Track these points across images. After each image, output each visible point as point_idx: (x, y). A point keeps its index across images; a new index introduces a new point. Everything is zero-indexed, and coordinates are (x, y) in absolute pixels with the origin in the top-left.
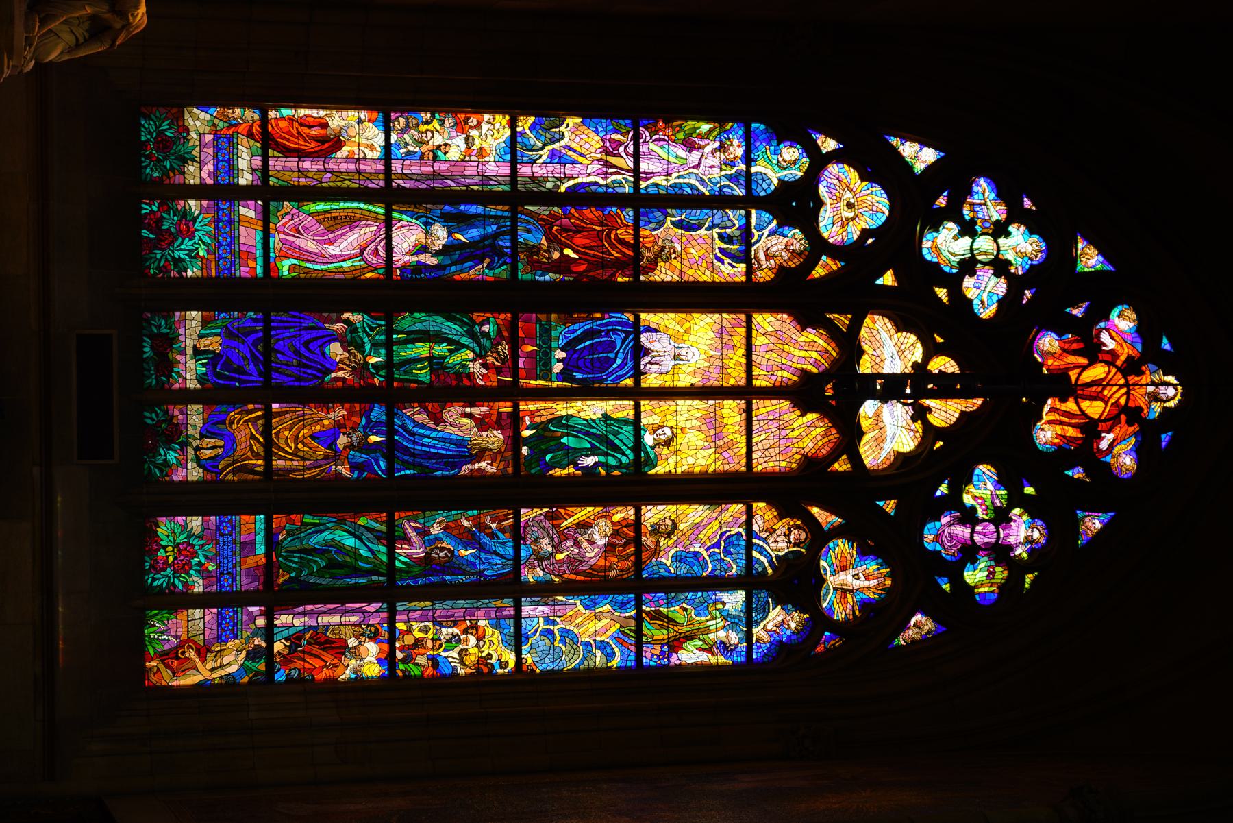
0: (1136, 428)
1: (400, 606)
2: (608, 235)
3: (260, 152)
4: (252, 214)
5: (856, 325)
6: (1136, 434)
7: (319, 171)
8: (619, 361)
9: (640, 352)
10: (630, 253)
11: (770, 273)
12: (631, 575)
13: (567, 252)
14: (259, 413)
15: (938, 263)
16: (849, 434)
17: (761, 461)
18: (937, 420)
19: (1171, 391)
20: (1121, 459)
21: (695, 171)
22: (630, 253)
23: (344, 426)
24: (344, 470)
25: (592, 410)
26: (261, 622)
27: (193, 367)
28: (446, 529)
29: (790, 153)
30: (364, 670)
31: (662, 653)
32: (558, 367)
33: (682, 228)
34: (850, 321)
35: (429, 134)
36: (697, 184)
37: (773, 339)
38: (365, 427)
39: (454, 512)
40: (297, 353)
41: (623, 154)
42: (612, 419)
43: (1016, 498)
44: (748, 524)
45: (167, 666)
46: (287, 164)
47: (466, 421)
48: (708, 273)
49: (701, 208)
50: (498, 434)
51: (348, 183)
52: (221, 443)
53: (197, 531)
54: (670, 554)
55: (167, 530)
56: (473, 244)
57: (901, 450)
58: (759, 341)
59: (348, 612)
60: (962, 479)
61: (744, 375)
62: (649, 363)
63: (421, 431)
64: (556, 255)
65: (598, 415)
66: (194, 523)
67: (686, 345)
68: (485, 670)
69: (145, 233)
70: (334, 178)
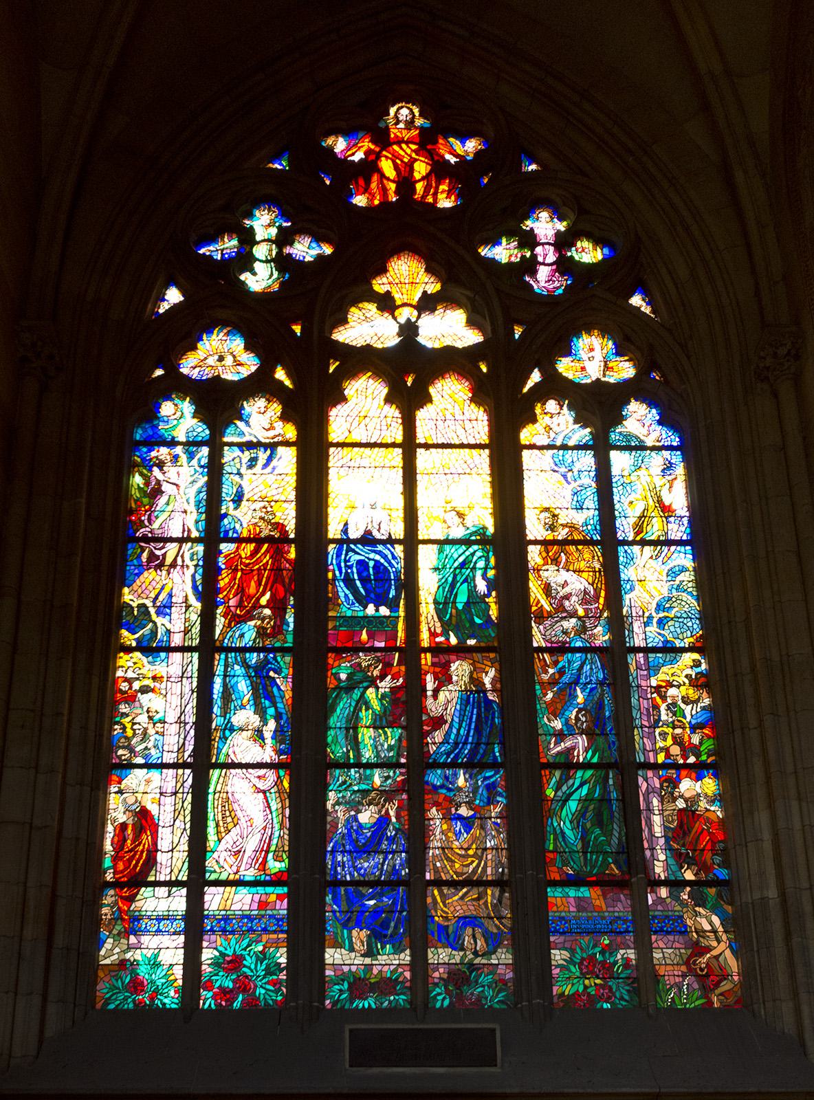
1: (641, 758)
6: (446, 138)
8: (378, 557)
9: (367, 539)
10: (266, 546)
13: (263, 601)
14: (436, 892)
17: (477, 436)
20: (469, 150)
22: (266, 546)
25: (428, 585)
27: (385, 957)
30: (710, 793)
32: (384, 611)
35: (135, 727)
38: (449, 790)
39: (538, 707)
41: (163, 551)
47: (442, 696)
50: (453, 667)
53: (566, 954)
57: (465, 320)
58: (359, 436)
62: (379, 530)
63: (453, 736)
64: (267, 612)
65: (436, 577)
67: (361, 497)
68: (702, 680)
69: (237, 1004)
70: (181, 817)
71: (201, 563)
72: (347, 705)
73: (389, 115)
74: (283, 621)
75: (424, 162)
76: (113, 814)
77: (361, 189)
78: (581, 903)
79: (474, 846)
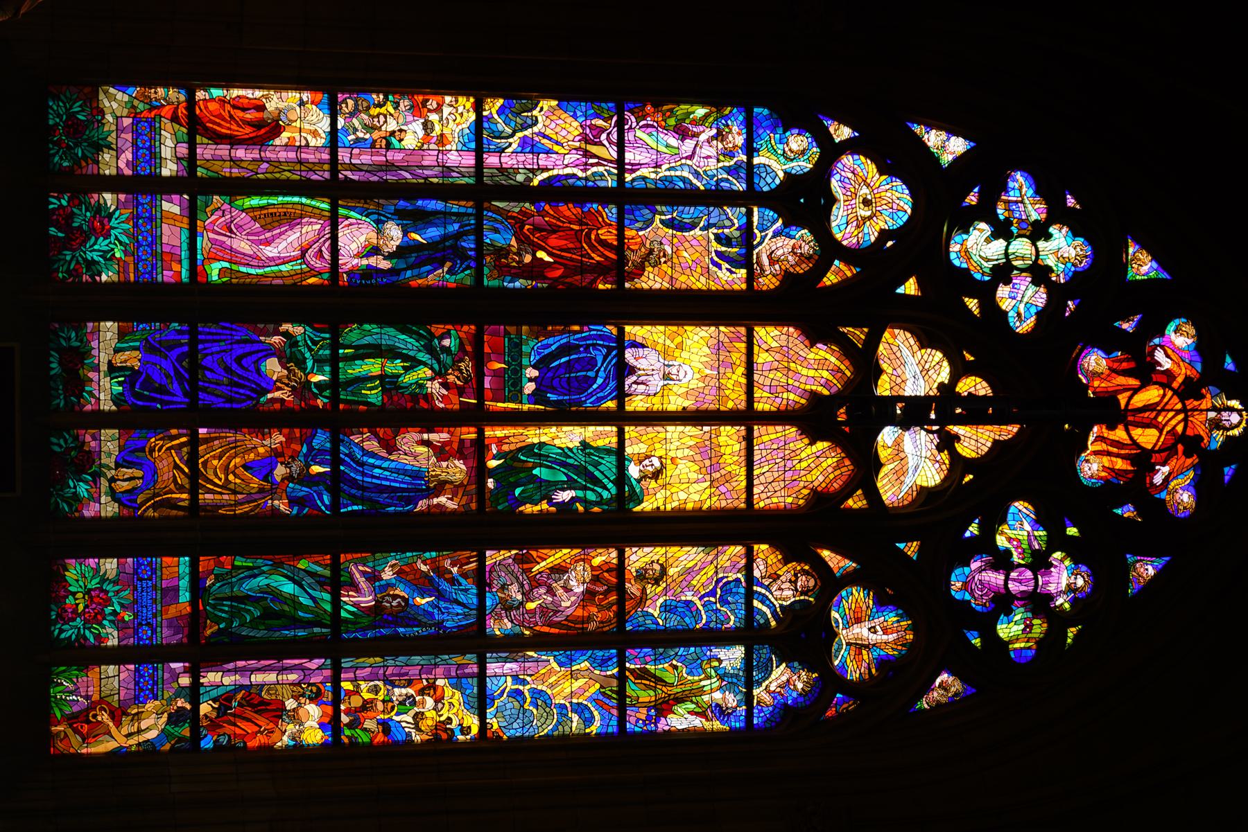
0: (1194, 459)
1: (346, 663)
2: (588, 235)
3: (186, 138)
4: (176, 210)
5: (874, 341)
7: (254, 160)
8: (600, 381)
9: (624, 370)
10: (613, 256)
11: (774, 280)
12: (613, 627)
13: (541, 254)
14: (184, 439)
15: (968, 270)
16: (865, 466)
17: (763, 496)
18: (966, 449)
19: (1235, 418)
20: (1178, 496)
21: (688, 162)
22: (613, 256)
23: (282, 454)
24: (282, 505)
25: (568, 437)
26: (185, 681)
27: (108, 386)
28: (400, 573)
29: (797, 142)
30: (304, 736)
31: (649, 717)
32: (529, 388)
33: (673, 228)
34: (867, 335)
35: (382, 119)
36: (691, 177)
37: (778, 357)
38: (306, 456)
39: (408, 554)
40: (228, 370)
41: (606, 143)
42: (592, 447)
43: (1057, 541)
44: (749, 568)
45: (76, 731)
46: (218, 152)
48: (703, 279)
49: (695, 205)
50: (460, 464)
51: (288, 174)
52: (139, 473)
54: (658, 604)
55: (76, 574)
56: (432, 245)
57: (925, 484)
58: (761, 358)
59: (286, 669)
60: (995, 518)
61: (743, 397)
62: (635, 383)
63: (371, 461)
64: (528, 259)
66: (108, 566)
67: (678, 363)
68: (444, 736)
69: (53, 231)
71: (590, 184)
72: (410, 347)
73: (1228, 398)
74: (515, 277)
75: (1158, 440)
76: (274, 96)
77: (1115, 365)
78: (171, 593)
79: (238, 481)
